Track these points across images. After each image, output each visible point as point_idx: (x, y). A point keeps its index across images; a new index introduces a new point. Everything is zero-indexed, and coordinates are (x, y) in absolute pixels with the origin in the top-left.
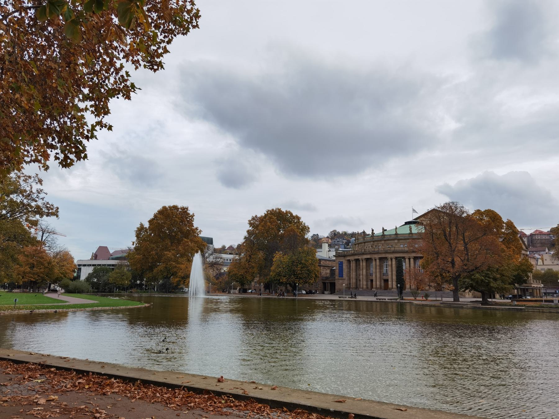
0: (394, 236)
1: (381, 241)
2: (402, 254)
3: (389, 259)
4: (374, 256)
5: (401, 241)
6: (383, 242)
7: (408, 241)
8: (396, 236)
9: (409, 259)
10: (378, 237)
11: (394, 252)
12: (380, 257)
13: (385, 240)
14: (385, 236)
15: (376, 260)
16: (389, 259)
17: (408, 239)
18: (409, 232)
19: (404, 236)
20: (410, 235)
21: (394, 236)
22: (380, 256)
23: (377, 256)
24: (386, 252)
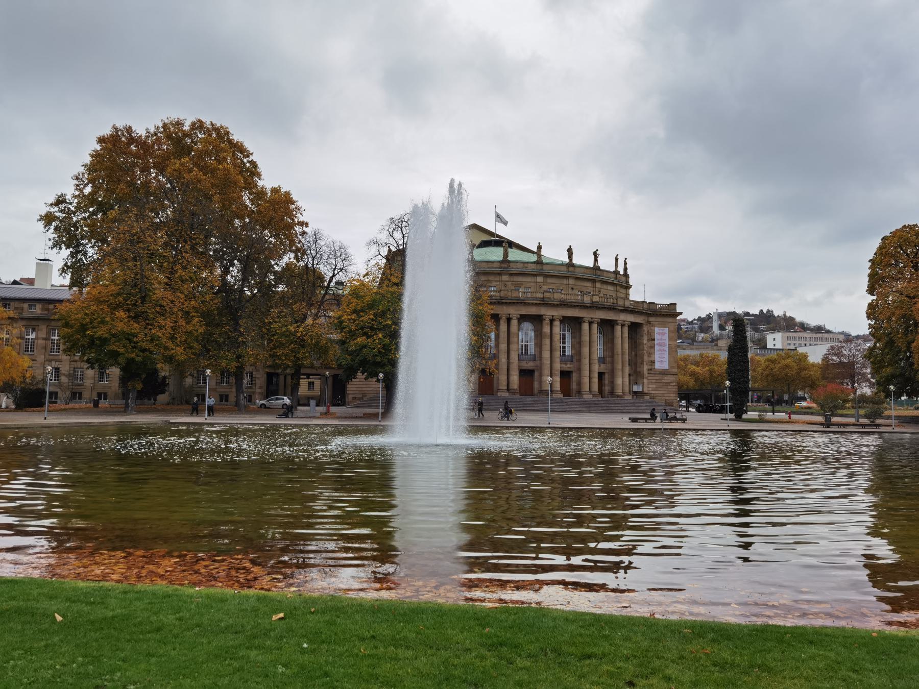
0: (534, 266)
1: (500, 274)
2: (577, 310)
3: (547, 321)
4: (503, 311)
5: (549, 280)
6: (505, 278)
7: (565, 281)
8: (539, 267)
9: (590, 323)
10: (490, 265)
11: (563, 304)
12: (524, 313)
13: (511, 275)
14: (511, 265)
15: (509, 320)
16: (547, 322)
17: (566, 277)
18: (567, 260)
19: (558, 268)
20: (571, 269)
21: (534, 266)
22: (524, 311)
23: (515, 312)
24: (544, 303)
